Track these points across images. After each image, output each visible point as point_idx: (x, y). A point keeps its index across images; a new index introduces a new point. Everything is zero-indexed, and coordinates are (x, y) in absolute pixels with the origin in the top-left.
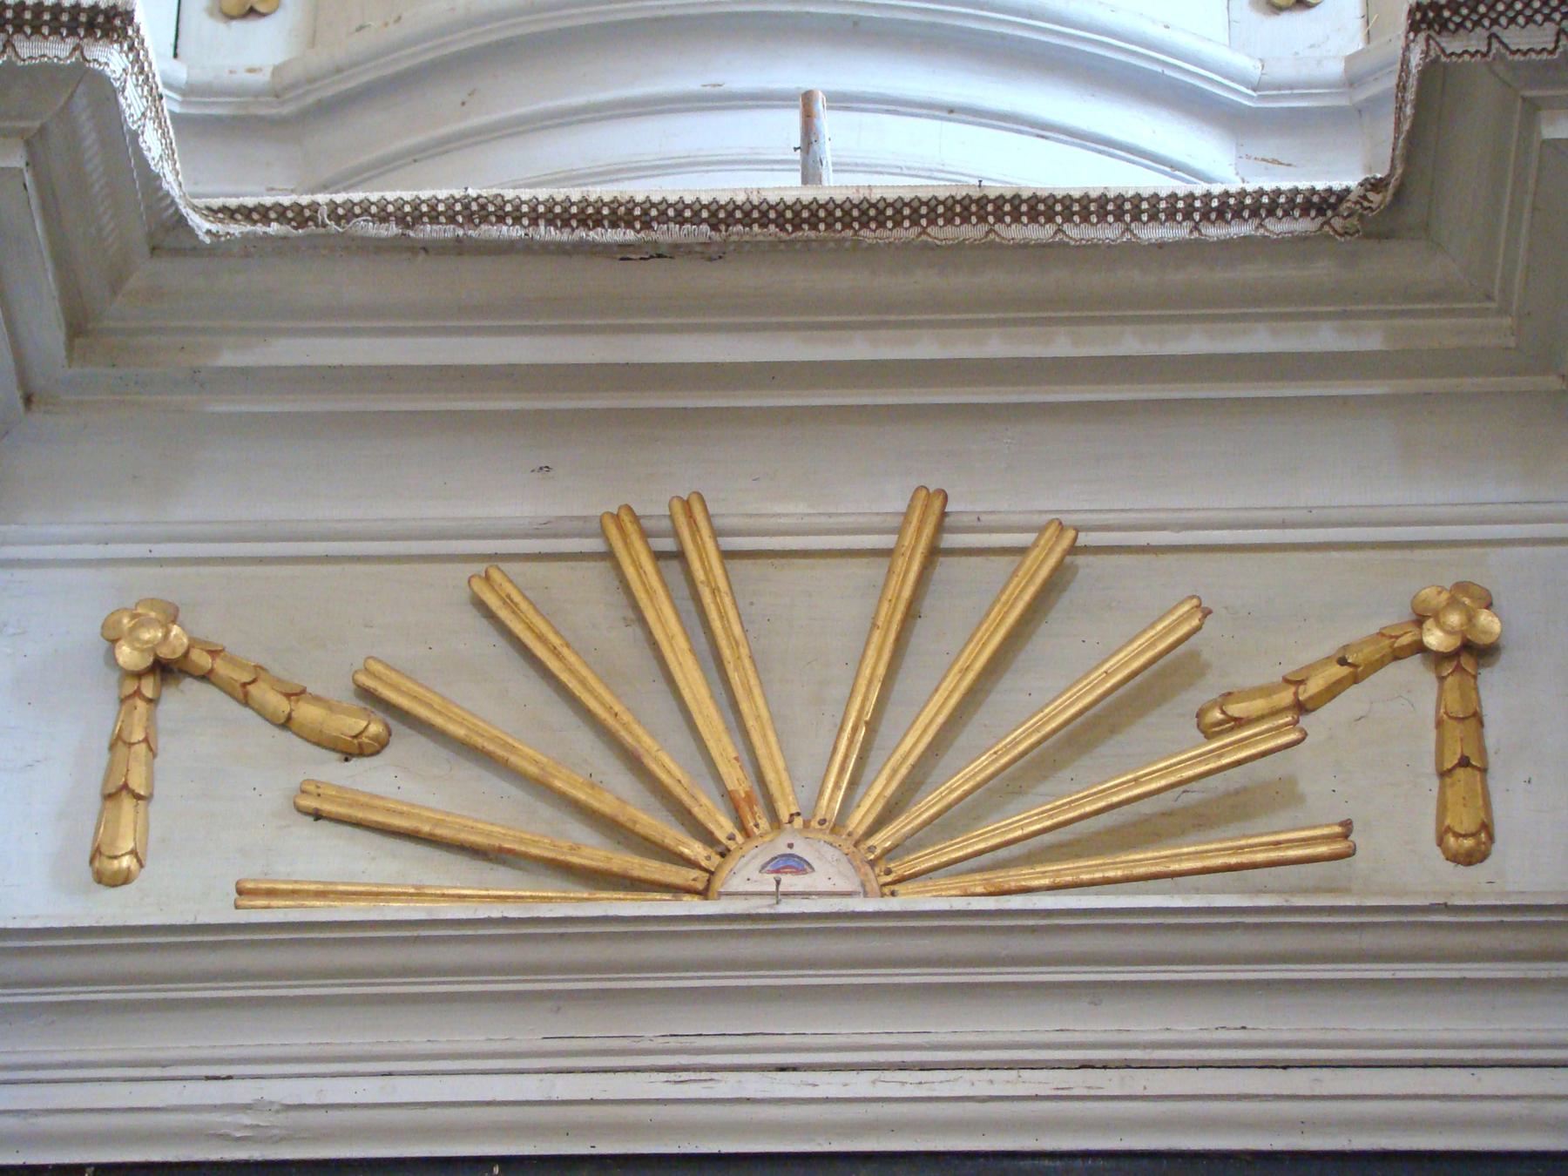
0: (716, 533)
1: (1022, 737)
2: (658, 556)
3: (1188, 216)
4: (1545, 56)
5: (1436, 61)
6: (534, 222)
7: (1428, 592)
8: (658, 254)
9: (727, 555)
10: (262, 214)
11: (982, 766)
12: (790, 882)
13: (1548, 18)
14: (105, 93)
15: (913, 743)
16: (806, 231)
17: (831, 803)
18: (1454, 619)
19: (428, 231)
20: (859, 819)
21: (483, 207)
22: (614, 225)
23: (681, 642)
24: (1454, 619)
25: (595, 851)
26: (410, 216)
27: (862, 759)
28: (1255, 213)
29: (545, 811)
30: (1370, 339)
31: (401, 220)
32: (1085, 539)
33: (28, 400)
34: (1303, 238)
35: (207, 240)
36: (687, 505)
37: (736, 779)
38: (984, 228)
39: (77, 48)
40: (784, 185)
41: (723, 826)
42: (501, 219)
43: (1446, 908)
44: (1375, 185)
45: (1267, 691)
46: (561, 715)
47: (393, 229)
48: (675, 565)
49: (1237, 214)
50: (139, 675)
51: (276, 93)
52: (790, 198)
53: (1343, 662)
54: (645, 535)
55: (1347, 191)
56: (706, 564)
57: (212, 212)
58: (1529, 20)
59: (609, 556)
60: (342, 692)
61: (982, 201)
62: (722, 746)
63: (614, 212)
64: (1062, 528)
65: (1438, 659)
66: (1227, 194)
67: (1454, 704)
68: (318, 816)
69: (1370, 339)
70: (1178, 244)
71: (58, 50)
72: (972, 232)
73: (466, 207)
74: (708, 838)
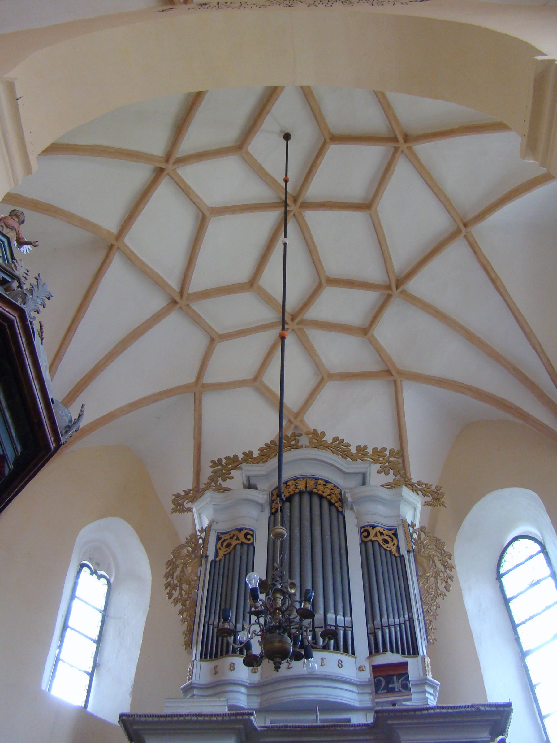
14: (251, 721)
30: (372, 738)
51: (258, 684)
69: (372, 738)
71: (247, 717)
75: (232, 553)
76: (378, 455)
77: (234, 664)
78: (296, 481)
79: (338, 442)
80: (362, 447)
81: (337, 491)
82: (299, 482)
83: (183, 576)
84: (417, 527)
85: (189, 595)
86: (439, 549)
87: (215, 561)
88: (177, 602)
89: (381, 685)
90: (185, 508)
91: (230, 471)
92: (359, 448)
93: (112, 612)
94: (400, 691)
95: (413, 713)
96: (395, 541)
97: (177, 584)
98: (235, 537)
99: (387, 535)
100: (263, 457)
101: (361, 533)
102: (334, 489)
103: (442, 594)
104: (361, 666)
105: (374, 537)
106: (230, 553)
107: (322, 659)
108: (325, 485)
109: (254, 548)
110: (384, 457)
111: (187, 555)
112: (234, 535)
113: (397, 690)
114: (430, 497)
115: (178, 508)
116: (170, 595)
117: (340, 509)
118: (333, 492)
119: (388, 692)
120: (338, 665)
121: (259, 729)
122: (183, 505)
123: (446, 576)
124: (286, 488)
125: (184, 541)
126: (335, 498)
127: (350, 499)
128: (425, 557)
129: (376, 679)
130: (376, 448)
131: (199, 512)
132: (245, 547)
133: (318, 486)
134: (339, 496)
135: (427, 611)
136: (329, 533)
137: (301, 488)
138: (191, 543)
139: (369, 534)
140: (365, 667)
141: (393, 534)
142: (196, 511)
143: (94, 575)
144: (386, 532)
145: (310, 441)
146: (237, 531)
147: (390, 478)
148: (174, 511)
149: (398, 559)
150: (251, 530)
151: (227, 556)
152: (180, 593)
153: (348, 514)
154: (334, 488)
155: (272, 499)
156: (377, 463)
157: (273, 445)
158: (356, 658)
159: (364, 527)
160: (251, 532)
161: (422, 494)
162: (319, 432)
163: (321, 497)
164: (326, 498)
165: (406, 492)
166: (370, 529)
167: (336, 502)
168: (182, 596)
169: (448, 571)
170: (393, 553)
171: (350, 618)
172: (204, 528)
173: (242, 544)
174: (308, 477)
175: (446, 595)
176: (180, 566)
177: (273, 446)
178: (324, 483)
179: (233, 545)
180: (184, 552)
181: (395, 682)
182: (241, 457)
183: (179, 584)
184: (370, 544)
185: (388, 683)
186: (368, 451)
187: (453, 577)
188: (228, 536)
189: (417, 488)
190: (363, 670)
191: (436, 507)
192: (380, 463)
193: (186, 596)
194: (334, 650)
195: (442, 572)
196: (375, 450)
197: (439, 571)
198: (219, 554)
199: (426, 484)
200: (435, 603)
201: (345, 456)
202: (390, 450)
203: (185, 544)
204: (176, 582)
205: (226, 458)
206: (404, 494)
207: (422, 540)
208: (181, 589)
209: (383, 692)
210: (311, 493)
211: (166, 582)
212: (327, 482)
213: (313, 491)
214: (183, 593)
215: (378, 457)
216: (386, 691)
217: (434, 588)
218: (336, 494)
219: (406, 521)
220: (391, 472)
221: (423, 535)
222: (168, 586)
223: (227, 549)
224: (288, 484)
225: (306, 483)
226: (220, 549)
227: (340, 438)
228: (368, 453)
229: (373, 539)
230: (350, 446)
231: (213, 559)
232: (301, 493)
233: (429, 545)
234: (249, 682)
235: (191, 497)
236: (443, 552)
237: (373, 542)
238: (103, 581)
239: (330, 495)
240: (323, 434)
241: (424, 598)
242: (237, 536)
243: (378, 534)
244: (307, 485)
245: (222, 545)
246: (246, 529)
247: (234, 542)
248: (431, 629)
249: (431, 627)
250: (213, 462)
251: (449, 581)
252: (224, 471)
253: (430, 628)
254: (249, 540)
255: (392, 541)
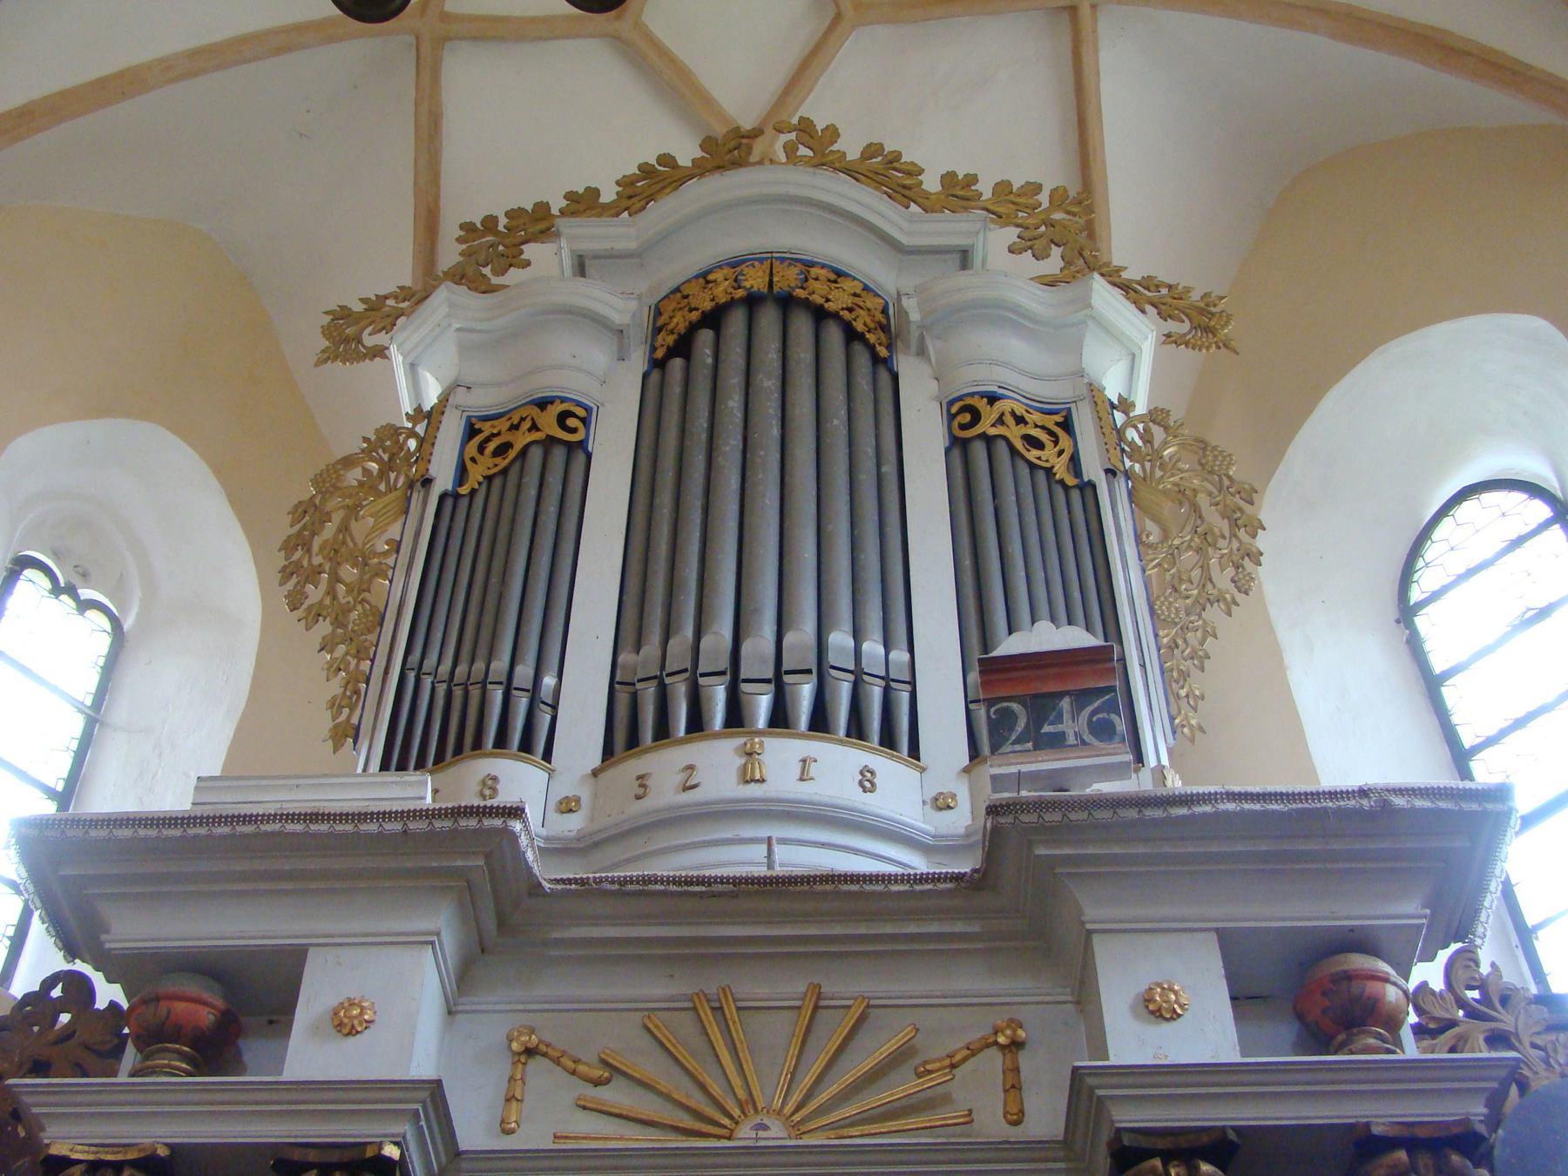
0: (735, 1000)
1: (849, 1078)
2: (713, 1009)
3: (908, 882)
4: (1034, 825)
5: (996, 826)
6: (668, 884)
7: (999, 1022)
8: (714, 895)
9: (738, 1009)
10: (569, 881)
11: (834, 1089)
12: (761, 1134)
13: (1035, 811)
14: (514, 838)
15: (808, 1080)
16: (768, 887)
17: (777, 1103)
18: (1008, 1032)
19: (630, 887)
20: (788, 1109)
21: (649, 878)
22: (698, 885)
23: (721, 1041)
24: (1008, 1032)
25: (688, 1122)
26: (624, 882)
27: (789, 1086)
28: (933, 881)
29: (669, 1106)
30: (975, 928)
31: (620, 883)
32: (872, 1002)
33: (483, 951)
34: (950, 891)
35: (549, 891)
36: (724, 990)
37: (742, 1094)
38: (834, 886)
39: (504, 821)
40: (761, 871)
41: (736, 1112)
42: (656, 883)
43: (1010, 1143)
44: (975, 871)
45: (939, 1060)
46: (676, 1070)
47: (616, 887)
48: (719, 1013)
49: (926, 881)
50: (520, 1054)
52: (762, 875)
53: (968, 1049)
54: (708, 1001)
55: (966, 873)
56: (731, 1011)
57: (551, 881)
58: (1029, 812)
59: (695, 1009)
60: (594, 1059)
61: (833, 876)
62: (736, 1081)
63: (697, 880)
64: (864, 998)
65: (1002, 1047)
66: (922, 874)
67: (1009, 1064)
68: (584, 1108)
69: (975, 928)
70: (904, 892)
71: (497, 822)
72: (829, 887)
73: (643, 878)
74: (731, 1117)
75: (513, 476)
76: (1013, 203)
77: (495, 779)
78: (738, 269)
79: (879, 159)
80: (960, 177)
81: (870, 302)
82: (746, 271)
83: (344, 543)
84: (1140, 409)
85: (359, 594)
86: (1211, 472)
87: (457, 497)
88: (319, 615)
89: (1011, 729)
90: (363, 346)
91: (522, 247)
92: (949, 179)
93: (120, 710)
94: (1084, 743)
95: (1132, 813)
96: (1065, 441)
97: (320, 565)
98: (527, 425)
99: (1036, 426)
100: (633, 200)
101: (952, 417)
102: (862, 295)
103: (1225, 599)
104: (941, 793)
105: (993, 425)
106: (505, 472)
107: (804, 761)
108: (835, 282)
109: (589, 456)
110: (1034, 209)
111: (361, 484)
112: (523, 419)
113: (1071, 740)
114: (1183, 322)
115: (341, 350)
116: (295, 599)
117: (883, 352)
118: (861, 304)
119: (1036, 748)
120: (861, 784)
121: (547, 885)
122: (360, 341)
123: (1239, 550)
124: (704, 288)
125: (355, 446)
126: (868, 320)
127: (914, 316)
128: (1165, 492)
129: (993, 710)
130: (1008, 184)
131: (410, 360)
132: (559, 454)
133: (811, 281)
134: (879, 317)
135: (1173, 645)
136: (843, 412)
137: (752, 287)
138: (380, 451)
139: (976, 417)
140: (954, 796)
141: (1057, 424)
142: (400, 358)
143: (64, 597)
144: (1035, 417)
145: (790, 150)
146: (534, 407)
147: (1053, 264)
148: (329, 358)
149: (1075, 496)
150: (579, 404)
151: (497, 482)
152: (331, 592)
153: (907, 366)
154: (864, 294)
155: (659, 323)
156: (1007, 225)
157: (665, 167)
158: (923, 770)
159: (960, 399)
160: (581, 413)
161: (1159, 314)
162: (819, 127)
163: (820, 315)
164: (835, 316)
165: (1103, 294)
166: (981, 404)
167: (869, 332)
168: (335, 598)
169: (1242, 533)
170: (1057, 476)
171: (906, 656)
172: (427, 407)
173: (551, 441)
174: (777, 258)
175: (1235, 603)
176: (337, 517)
177: (666, 169)
178: (833, 277)
179: (518, 447)
180: (354, 476)
181: (1066, 716)
182: (557, 204)
183: (327, 568)
184: (979, 450)
185: (1037, 720)
186: (980, 190)
187: (1261, 554)
188: (503, 425)
189: (1142, 294)
190: (949, 807)
191: (1204, 351)
192: (1017, 226)
193: (350, 599)
194: (848, 735)
195: (1223, 537)
196: (1003, 188)
197: (1213, 534)
198: (471, 475)
199: (1170, 287)
200: (1200, 622)
201: (906, 200)
202: (1054, 192)
203: (360, 454)
204: (317, 560)
205: (507, 214)
206: (1096, 300)
207: (1156, 447)
208: (336, 578)
209: (1018, 747)
210: (787, 303)
211: (286, 563)
212: (839, 274)
213: (795, 294)
214: (341, 588)
215: (1015, 207)
216: (1030, 745)
217: (1196, 582)
218: (869, 310)
219: (1101, 390)
220: (1056, 252)
221: (1158, 433)
222: (292, 574)
223: (498, 460)
224: (711, 277)
225: (771, 274)
226: (473, 460)
227: (887, 149)
228: (981, 194)
229: (993, 431)
230: (921, 172)
231: (450, 487)
232: (752, 302)
233: (1178, 461)
234: (544, 832)
235: (388, 316)
236: (1226, 482)
237: (989, 440)
238: (92, 614)
239: (850, 310)
240: (833, 133)
241: (1160, 607)
242: (533, 419)
243: (1009, 420)
244: (775, 279)
245: (481, 449)
246: (562, 402)
247: (521, 439)
248: (1187, 696)
249: (1185, 690)
250: (468, 228)
251: (1247, 562)
252: (501, 248)
253: (1183, 693)
254: (574, 431)
255: (1056, 443)
